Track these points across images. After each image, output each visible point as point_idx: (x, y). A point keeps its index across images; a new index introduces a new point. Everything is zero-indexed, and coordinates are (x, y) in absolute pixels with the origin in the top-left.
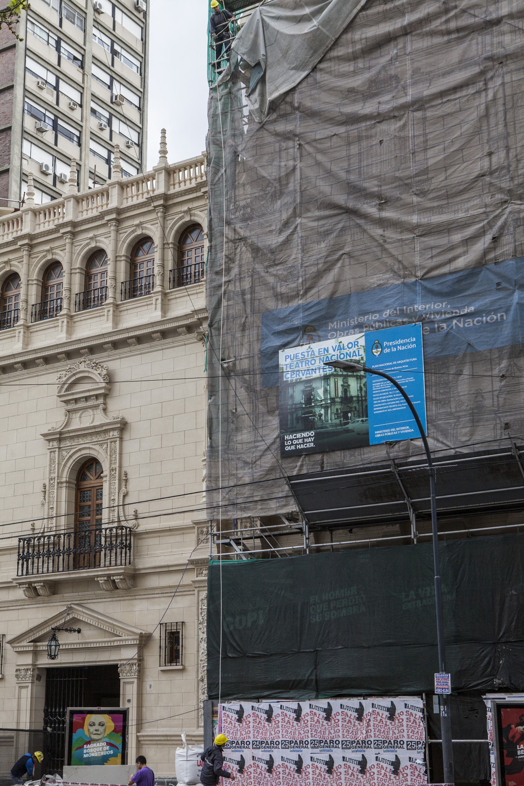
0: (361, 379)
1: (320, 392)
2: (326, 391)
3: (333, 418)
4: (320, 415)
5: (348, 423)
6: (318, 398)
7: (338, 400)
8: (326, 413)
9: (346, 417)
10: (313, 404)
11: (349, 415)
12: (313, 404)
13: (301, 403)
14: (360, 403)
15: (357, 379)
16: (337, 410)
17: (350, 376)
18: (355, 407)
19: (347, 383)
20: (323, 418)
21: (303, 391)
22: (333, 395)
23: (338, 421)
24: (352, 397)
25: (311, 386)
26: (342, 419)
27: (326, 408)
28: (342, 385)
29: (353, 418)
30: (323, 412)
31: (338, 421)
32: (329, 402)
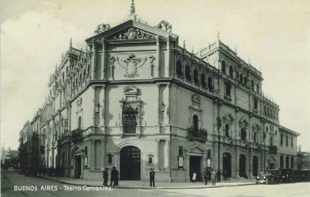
0: (219, 105)
15: (214, 103)
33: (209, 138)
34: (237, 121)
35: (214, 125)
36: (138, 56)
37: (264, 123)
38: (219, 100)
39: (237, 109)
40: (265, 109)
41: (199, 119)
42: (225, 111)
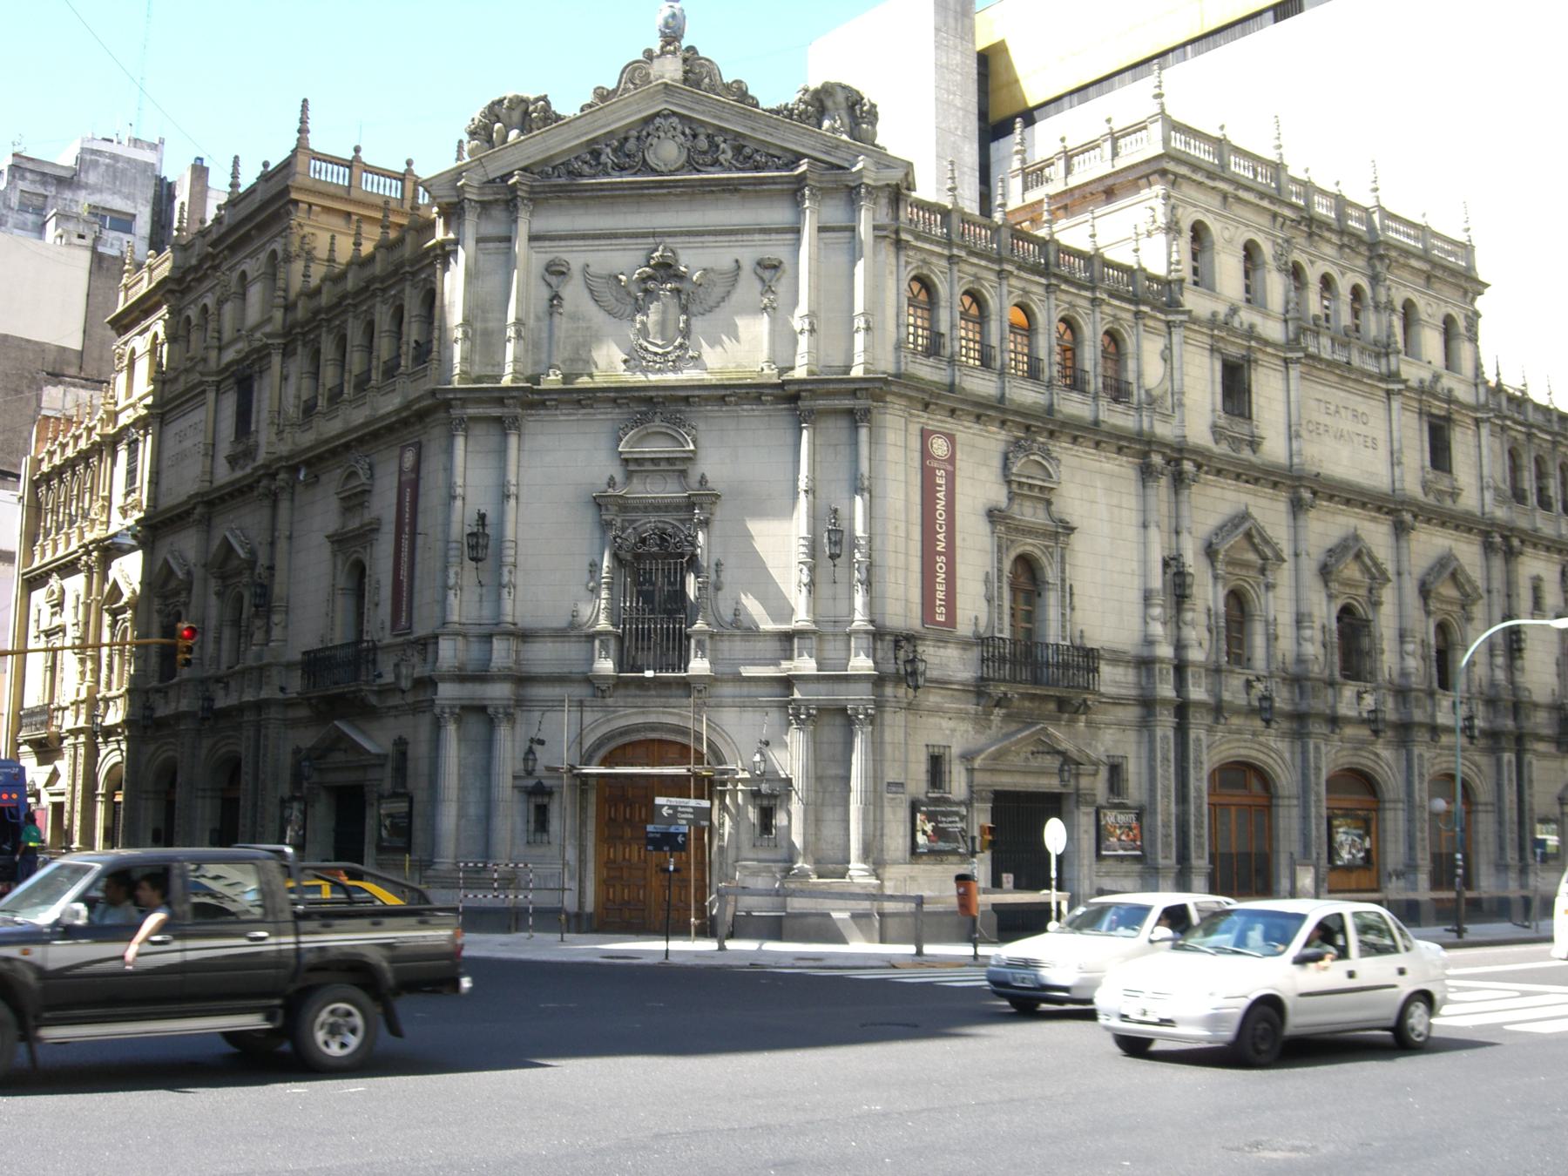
0: (1179, 481)
1: (782, 543)
2: (830, 547)
3: (896, 841)
4: (768, 800)
5: (1031, 921)
6: (753, 607)
7: (949, 662)
8: (829, 781)
9: (1018, 854)
10: (699, 666)
11: (1055, 835)
12: (699, 666)
13: (573, 632)
14: (1165, 724)
15: (1147, 473)
16: (936, 766)
17: (1091, 434)
18: (1116, 771)
19: (1045, 496)
20: (794, 821)
21: (606, 508)
22: (903, 609)
23: (935, 884)
24: (1088, 658)
25: (679, 466)
26: (981, 868)
27: (832, 721)
28: (994, 516)
29: (1085, 872)
30: (792, 757)
31: (935, 884)
32: (861, 663)
33: (1113, 679)
34: (1310, 566)
35: (1147, 597)
36: (692, 260)
37: (1511, 554)
38: (1178, 452)
39: (1303, 489)
40: (1541, 475)
41: (1051, 574)
42: (1214, 503)
